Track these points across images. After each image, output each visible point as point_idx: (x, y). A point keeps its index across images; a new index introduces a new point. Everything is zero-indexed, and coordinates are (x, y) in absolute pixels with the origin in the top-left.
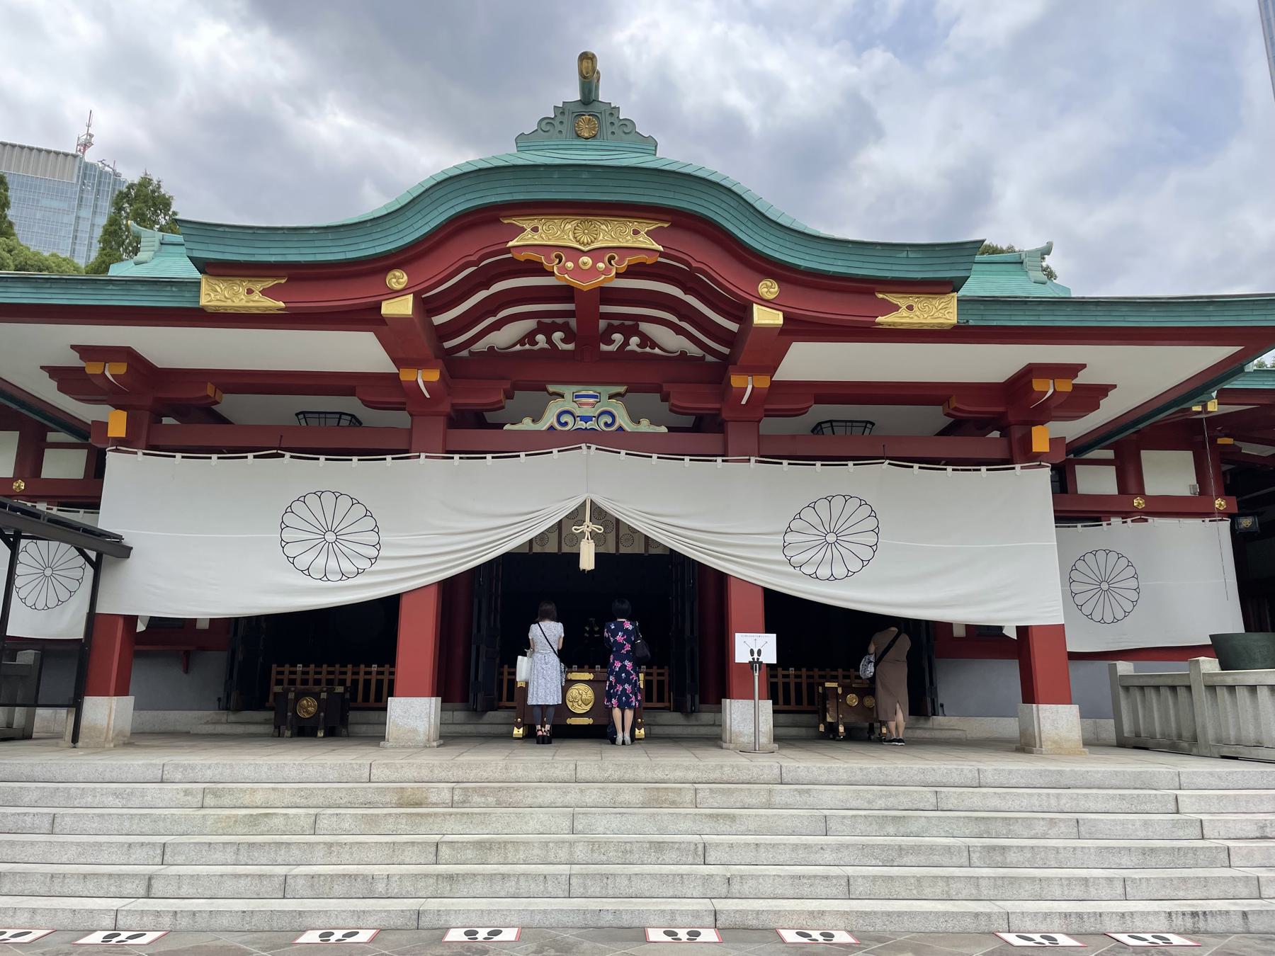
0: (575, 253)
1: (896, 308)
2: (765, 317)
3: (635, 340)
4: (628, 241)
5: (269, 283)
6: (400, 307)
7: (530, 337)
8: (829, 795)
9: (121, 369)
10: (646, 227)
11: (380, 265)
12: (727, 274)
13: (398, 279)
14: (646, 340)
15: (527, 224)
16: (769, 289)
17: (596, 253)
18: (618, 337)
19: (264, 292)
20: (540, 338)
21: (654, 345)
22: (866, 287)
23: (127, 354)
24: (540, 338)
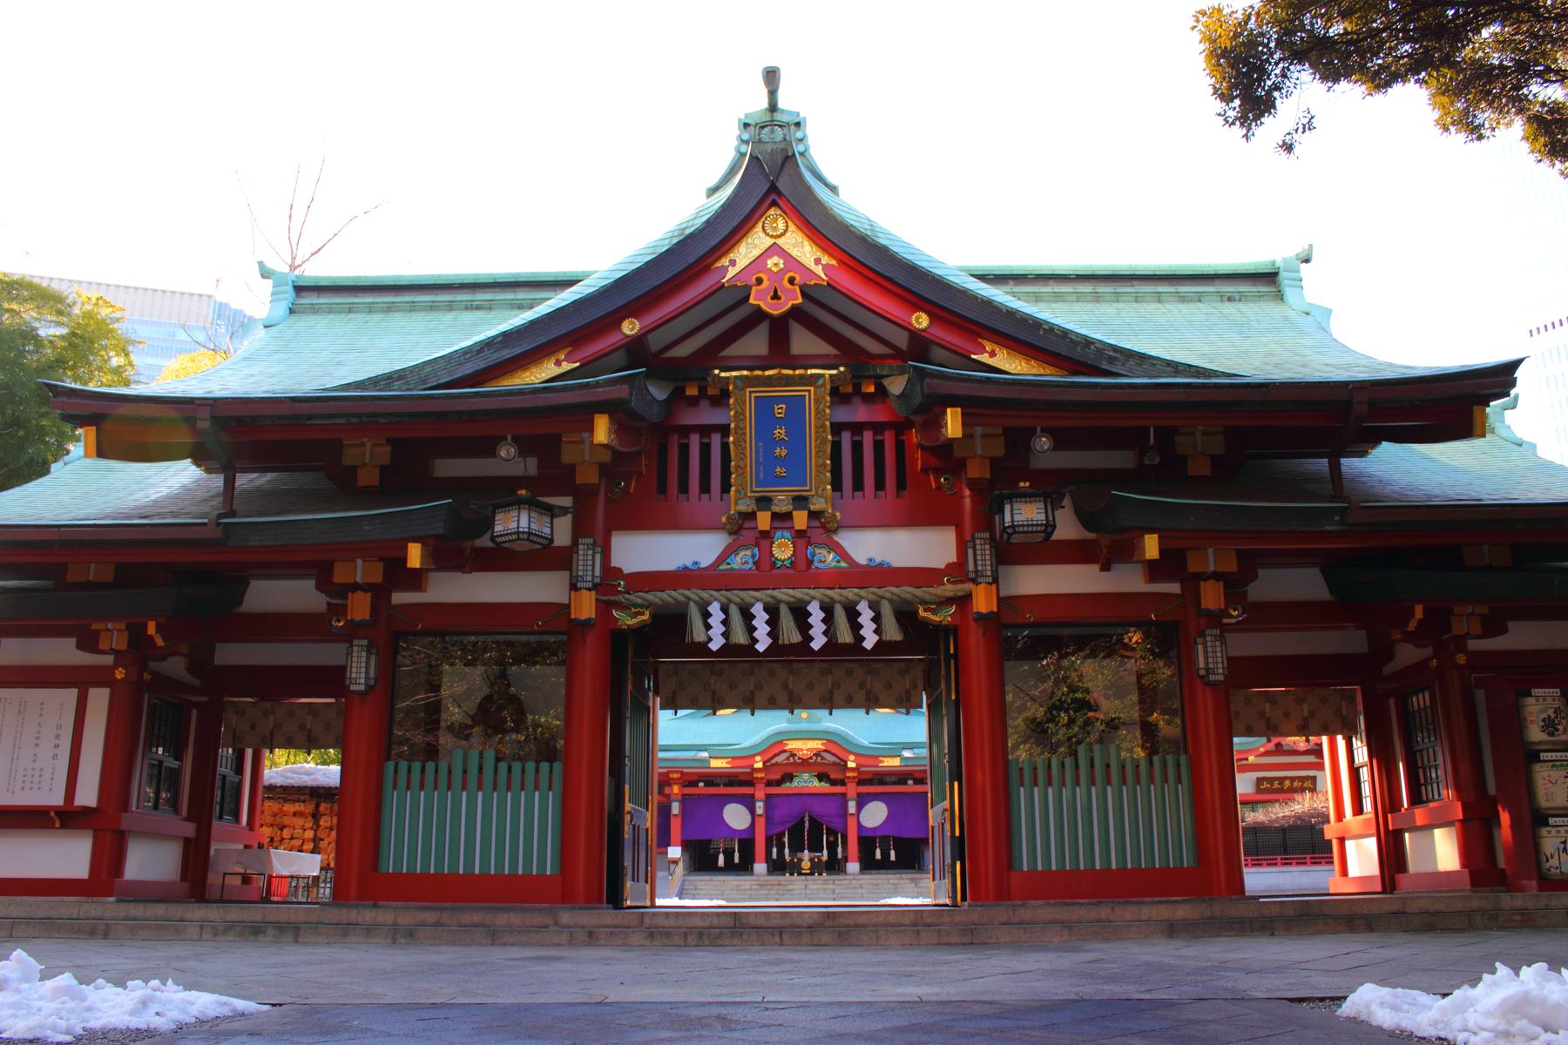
0: (802, 750)
1: (883, 762)
2: (851, 765)
3: (819, 758)
4: (816, 746)
5: (727, 760)
6: (759, 765)
7: (788, 758)
8: (862, 882)
9: (679, 776)
10: (820, 742)
11: (753, 756)
12: (840, 754)
13: (758, 758)
14: (823, 758)
15: (790, 742)
16: (852, 757)
17: (808, 750)
18: (814, 758)
19: (727, 763)
20: (791, 758)
21: (825, 759)
22: (877, 757)
23: (682, 773)
24: (791, 758)
